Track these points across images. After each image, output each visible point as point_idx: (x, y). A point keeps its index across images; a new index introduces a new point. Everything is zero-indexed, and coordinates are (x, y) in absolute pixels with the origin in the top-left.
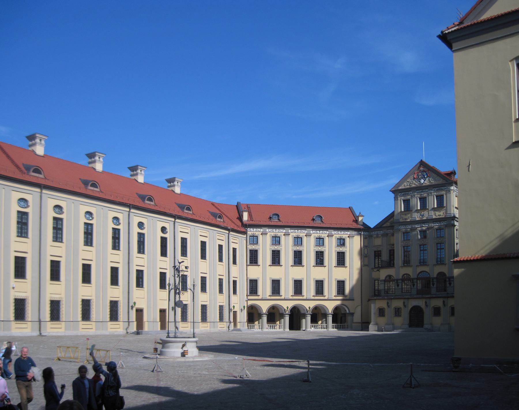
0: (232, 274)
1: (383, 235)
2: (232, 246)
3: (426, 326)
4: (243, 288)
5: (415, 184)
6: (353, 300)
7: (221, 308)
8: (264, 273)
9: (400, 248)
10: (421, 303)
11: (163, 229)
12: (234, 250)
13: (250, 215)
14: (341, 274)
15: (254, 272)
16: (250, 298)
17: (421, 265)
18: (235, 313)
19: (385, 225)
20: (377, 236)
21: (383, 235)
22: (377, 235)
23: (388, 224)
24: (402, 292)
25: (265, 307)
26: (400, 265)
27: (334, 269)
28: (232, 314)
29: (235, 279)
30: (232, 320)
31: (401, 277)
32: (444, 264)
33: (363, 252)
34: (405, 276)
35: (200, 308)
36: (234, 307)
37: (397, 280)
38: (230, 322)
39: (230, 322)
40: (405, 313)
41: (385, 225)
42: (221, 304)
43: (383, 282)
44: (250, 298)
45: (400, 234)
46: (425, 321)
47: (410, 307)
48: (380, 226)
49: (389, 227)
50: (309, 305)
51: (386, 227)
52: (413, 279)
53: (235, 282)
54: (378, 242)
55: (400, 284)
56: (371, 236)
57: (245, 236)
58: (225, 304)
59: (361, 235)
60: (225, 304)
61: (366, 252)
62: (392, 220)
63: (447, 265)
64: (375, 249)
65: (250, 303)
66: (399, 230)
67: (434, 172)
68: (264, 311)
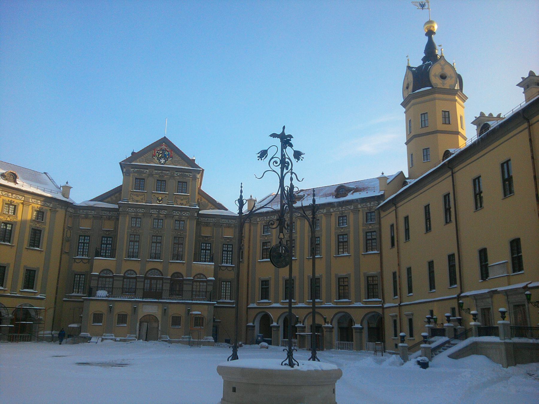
14: (33, 259)
45: (127, 219)
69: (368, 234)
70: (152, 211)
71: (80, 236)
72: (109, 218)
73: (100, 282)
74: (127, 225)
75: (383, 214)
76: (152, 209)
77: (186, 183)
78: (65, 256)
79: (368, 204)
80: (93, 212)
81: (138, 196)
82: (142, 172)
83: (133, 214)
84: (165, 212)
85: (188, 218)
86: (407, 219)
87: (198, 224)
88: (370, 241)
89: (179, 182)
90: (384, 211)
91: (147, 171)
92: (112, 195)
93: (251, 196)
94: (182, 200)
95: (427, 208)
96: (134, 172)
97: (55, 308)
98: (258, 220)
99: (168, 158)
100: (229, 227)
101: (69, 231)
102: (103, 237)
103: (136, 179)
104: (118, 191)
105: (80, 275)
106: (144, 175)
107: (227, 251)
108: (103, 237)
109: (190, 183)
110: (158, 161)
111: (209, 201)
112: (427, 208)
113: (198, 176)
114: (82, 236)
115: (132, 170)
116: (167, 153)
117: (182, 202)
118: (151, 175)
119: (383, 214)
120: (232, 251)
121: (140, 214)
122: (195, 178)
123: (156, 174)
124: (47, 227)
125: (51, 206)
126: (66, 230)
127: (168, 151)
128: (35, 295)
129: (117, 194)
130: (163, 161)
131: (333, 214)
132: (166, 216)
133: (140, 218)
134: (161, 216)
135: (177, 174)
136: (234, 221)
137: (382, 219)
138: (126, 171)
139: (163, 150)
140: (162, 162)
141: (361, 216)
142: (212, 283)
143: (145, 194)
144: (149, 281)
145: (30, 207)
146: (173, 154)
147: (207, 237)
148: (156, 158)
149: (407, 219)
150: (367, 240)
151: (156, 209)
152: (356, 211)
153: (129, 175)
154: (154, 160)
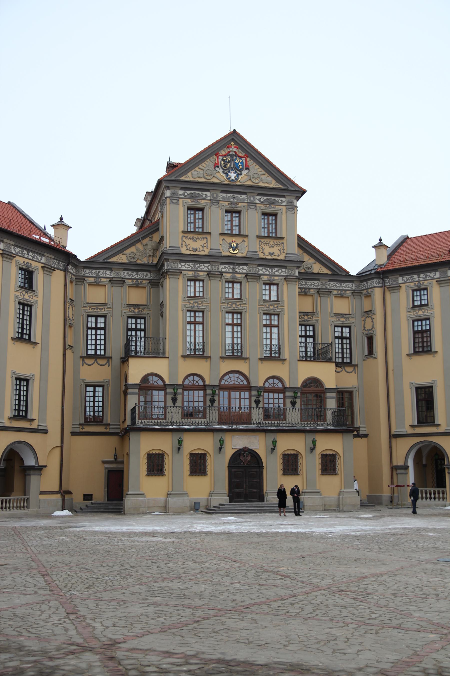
1: (112, 281)
5: (220, 176)
6: (45, 432)
9: (180, 314)
10: (257, 444)
17: (228, 357)
20: (97, 284)
21: (112, 281)
22: (98, 277)
23: (123, 258)
26: (181, 353)
32: (279, 359)
33: (67, 316)
34: (191, 378)
37: (175, 387)
41: (114, 260)
43: (137, 390)
47: (229, 452)
48: (101, 261)
52: (213, 387)
54: (96, 295)
55: (179, 397)
56: (81, 280)
59: (65, 270)
62: (133, 249)
63: (287, 363)
64: (91, 311)
66: (180, 272)
70: (223, 268)
74: (181, 294)
76: (222, 263)
77: (275, 215)
80: (108, 272)
81: (195, 241)
82: (199, 197)
83: (190, 273)
84: (244, 270)
85: (286, 278)
91: (208, 194)
92: (138, 241)
93: (380, 240)
94: (272, 247)
96: (186, 197)
97: (62, 447)
99: (241, 170)
100: (342, 296)
101: (71, 307)
102: (128, 317)
105: (95, 386)
106: (203, 202)
108: (128, 317)
109: (284, 216)
110: (224, 175)
114: (92, 316)
115: (181, 192)
116: (238, 160)
117: (272, 250)
118: (214, 201)
120: (350, 338)
121: (201, 274)
124: (40, 300)
125: (43, 260)
127: (241, 157)
128: (31, 424)
129: (146, 241)
130: (233, 175)
133: (203, 281)
134: (239, 276)
135: (259, 200)
136: (350, 285)
138: (172, 194)
139: (232, 156)
140: (233, 178)
143: (208, 237)
144: (226, 393)
146: (251, 163)
148: (221, 171)
153: (177, 203)
154: (217, 174)
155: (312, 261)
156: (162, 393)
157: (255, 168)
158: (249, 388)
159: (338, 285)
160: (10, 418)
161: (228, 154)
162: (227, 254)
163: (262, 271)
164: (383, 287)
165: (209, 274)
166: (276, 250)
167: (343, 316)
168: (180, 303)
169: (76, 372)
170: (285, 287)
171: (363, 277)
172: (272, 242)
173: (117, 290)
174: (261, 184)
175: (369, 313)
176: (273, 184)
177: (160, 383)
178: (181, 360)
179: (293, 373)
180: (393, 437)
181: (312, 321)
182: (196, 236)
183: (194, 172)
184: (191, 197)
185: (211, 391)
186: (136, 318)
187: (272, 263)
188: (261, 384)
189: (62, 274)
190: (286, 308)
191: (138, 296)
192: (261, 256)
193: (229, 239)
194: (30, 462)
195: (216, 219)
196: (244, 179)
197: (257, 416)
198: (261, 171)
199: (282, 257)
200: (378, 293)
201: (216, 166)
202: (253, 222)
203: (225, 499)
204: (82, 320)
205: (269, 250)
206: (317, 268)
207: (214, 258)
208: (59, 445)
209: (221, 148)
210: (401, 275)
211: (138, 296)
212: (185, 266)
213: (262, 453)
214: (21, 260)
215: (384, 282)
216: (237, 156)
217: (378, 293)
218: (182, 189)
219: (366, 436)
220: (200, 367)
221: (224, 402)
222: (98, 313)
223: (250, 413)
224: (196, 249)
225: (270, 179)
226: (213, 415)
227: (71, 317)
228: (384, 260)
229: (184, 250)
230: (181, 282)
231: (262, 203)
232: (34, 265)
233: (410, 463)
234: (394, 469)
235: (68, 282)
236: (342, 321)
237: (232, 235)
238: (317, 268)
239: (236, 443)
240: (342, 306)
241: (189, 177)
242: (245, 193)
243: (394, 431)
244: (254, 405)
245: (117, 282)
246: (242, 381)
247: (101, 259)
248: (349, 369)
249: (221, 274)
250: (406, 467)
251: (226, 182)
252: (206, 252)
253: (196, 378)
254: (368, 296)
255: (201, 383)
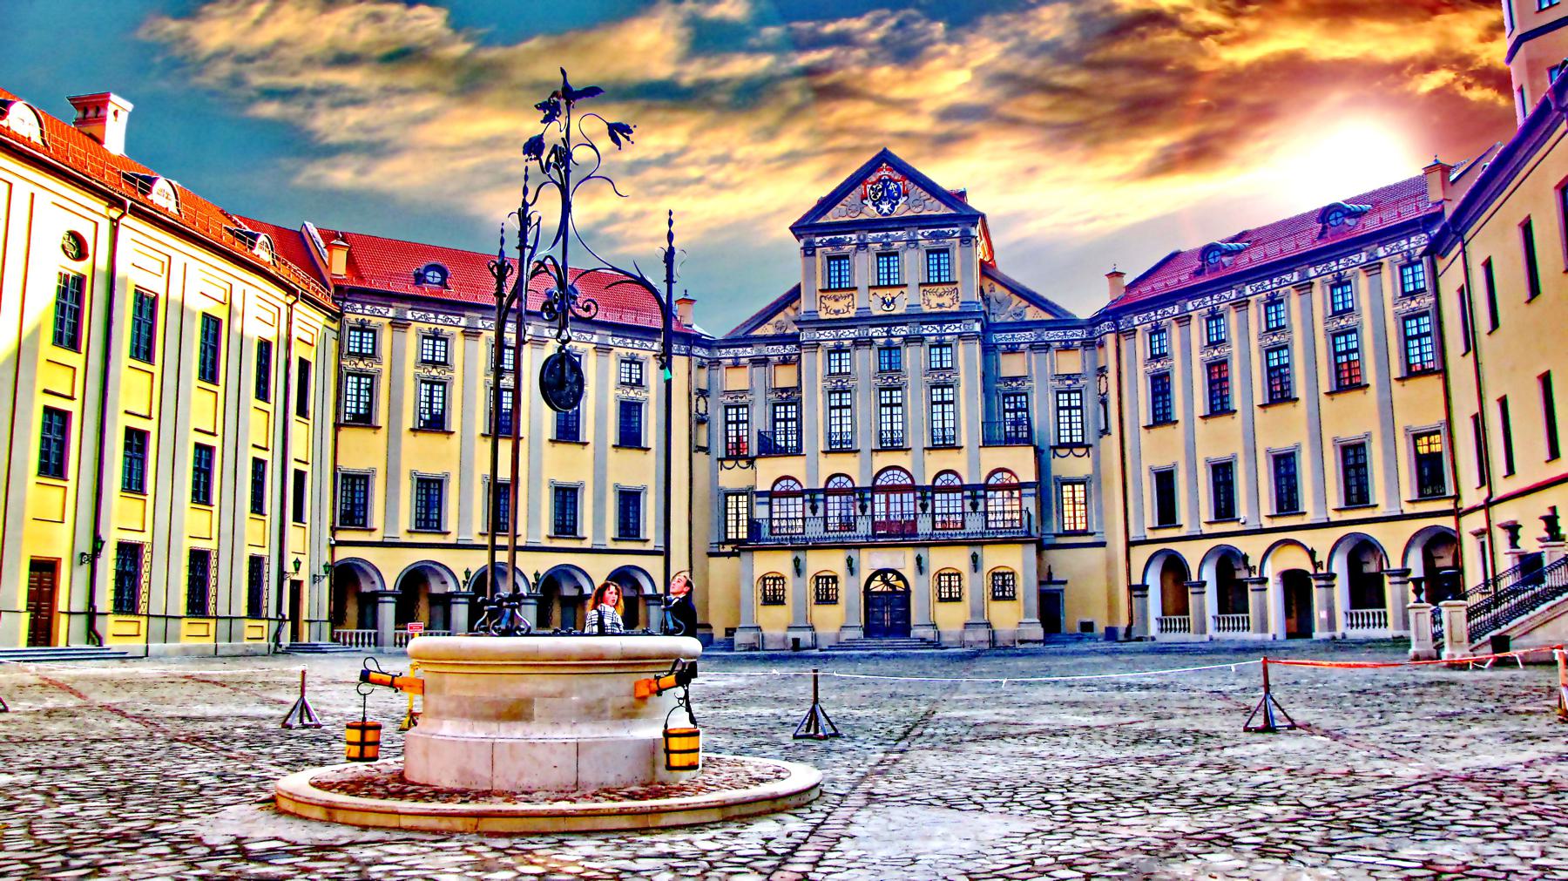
0: (298, 449)
2: (298, 351)
3: (917, 632)
4: (321, 499)
5: (871, 212)
7: (256, 563)
8: (391, 456)
11: (78, 246)
12: (304, 365)
13: (351, 262)
15: (362, 451)
16: (342, 536)
18: (296, 585)
19: (757, 332)
20: (736, 365)
22: (737, 358)
23: (768, 330)
24: (826, 530)
25: (391, 567)
26: (821, 448)
27: (611, 453)
28: (287, 585)
29: (302, 467)
30: (286, 610)
31: (822, 486)
34: (837, 480)
35: (185, 561)
36: (297, 563)
37: (813, 492)
38: (284, 620)
39: (284, 620)
40: (850, 591)
41: (757, 332)
42: (258, 552)
44: (342, 536)
45: (820, 356)
46: (915, 618)
49: (773, 337)
50: (533, 566)
51: (764, 338)
52: (862, 490)
53: (300, 476)
54: (736, 380)
55: (821, 505)
56: (716, 362)
57: (335, 326)
58: (269, 553)
59: (689, 354)
60: (269, 553)
61: (702, 410)
62: (780, 317)
65: (343, 553)
67: (920, 185)
68: (390, 586)
69: (1408, 324)
70: (873, 332)
71: (727, 407)
72: (785, 361)
73: (776, 508)
75: (1441, 264)
77: (946, 251)
78: (699, 457)
79: (1404, 242)
84: (905, 330)
86: (1488, 265)
87: (988, 350)
88: (1416, 343)
89: (929, 252)
90: (1443, 256)
91: (854, 236)
92: (785, 306)
95: (1526, 227)
98: (1136, 322)
103: (830, 258)
104: (795, 294)
106: (847, 248)
107: (1070, 408)
108: (775, 405)
111: (1013, 291)
112: (1526, 227)
113: (976, 231)
115: (818, 239)
116: (892, 186)
117: (940, 301)
118: (862, 245)
119: (1441, 264)
120: (1080, 408)
121: (846, 343)
122: (966, 239)
123: (875, 241)
126: (694, 397)
127: (895, 182)
129: (795, 305)
131: (1317, 281)
132: (905, 337)
134: (896, 340)
136: (1079, 332)
137: (1441, 280)
139: (885, 181)
141: (1388, 277)
142: (1033, 491)
145: (612, 355)
147: (1015, 379)
148: (870, 203)
149: (1488, 265)
150: (1407, 339)
151: (882, 326)
152: (1373, 267)
153: (814, 254)
155: (1025, 303)
156: (799, 500)
157: (917, 192)
158: (912, 488)
159: (1061, 333)
160: (615, 540)
161: (879, 180)
162: (882, 313)
163: (927, 329)
164: (1119, 333)
165: (857, 343)
166: (946, 300)
167: (1069, 377)
168: (820, 384)
169: (714, 478)
170: (961, 348)
171: (1094, 322)
172: (940, 289)
173: (759, 371)
174: (925, 213)
175: (1102, 371)
176: (943, 210)
177: (797, 488)
178: (821, 456)
179: (975, 463)
180: (1130, 544)
181: (1023, 388)
182: (838, 294)
183: (834, 210)
184: (830, 243)
185: (861, 495)
186: (786, 405)
187: (941, 318)
188: (929, 482)
189: (686, 359)
190: (962, 376)
191: (785, 377)
192: (926, 310)
193: (881, 293)
194: (648, 590)
195: (863, 268)
196: (901, 210)
197: (924, 526)
198: (925, 195)
199: (955, 308)
200: (1110, 339)
201: (864, 197)
202: (912, 264)
203: (859, 633)
204: (720, 413)
205: (935, 302)
206: (1032, 314)
207: (864, 319)
208: (687, 567)
209: (870, 173)
210: (1137, 313)
211: (785, 377)
212: (827, 334)
213: (909, 572)
214: (623, 352)
215: (1117, 326)
216: (891, 180)
217: (1110, 339)
218: (818, 235)
219: (1103, 544)
220: (846, 464)
221: (880, 508)
222: (738, 401)
223: (914, 524)
224: (837, 312)
225: (937, 202)
226: (864, 527)
227: (702, 410)
228: (1122, 292)
229: (823, 315)
230: (820, 356)
231: (926, 238)
232: (642, 354)
233: (1153, 580)
234: (1131, 588)
235: (694, 369)
236: (1069, 384)
237: (889, 286)
238: (1032, 314)
239: (871, 560)
240: (1071, 363)
241: (831, 217)
242: (902, 229)
243: (1133, 536)
244: (919, 510)
245: (763, 361)
246: (903, 480)
247: (740, 334)
248: (1081, 451)
249: (870, 342)
250: (1144, 587)
251: (879, 217)
252: (852, 313)
253: (844, 479)
254: (1102, 345)
255: (849, 485)
